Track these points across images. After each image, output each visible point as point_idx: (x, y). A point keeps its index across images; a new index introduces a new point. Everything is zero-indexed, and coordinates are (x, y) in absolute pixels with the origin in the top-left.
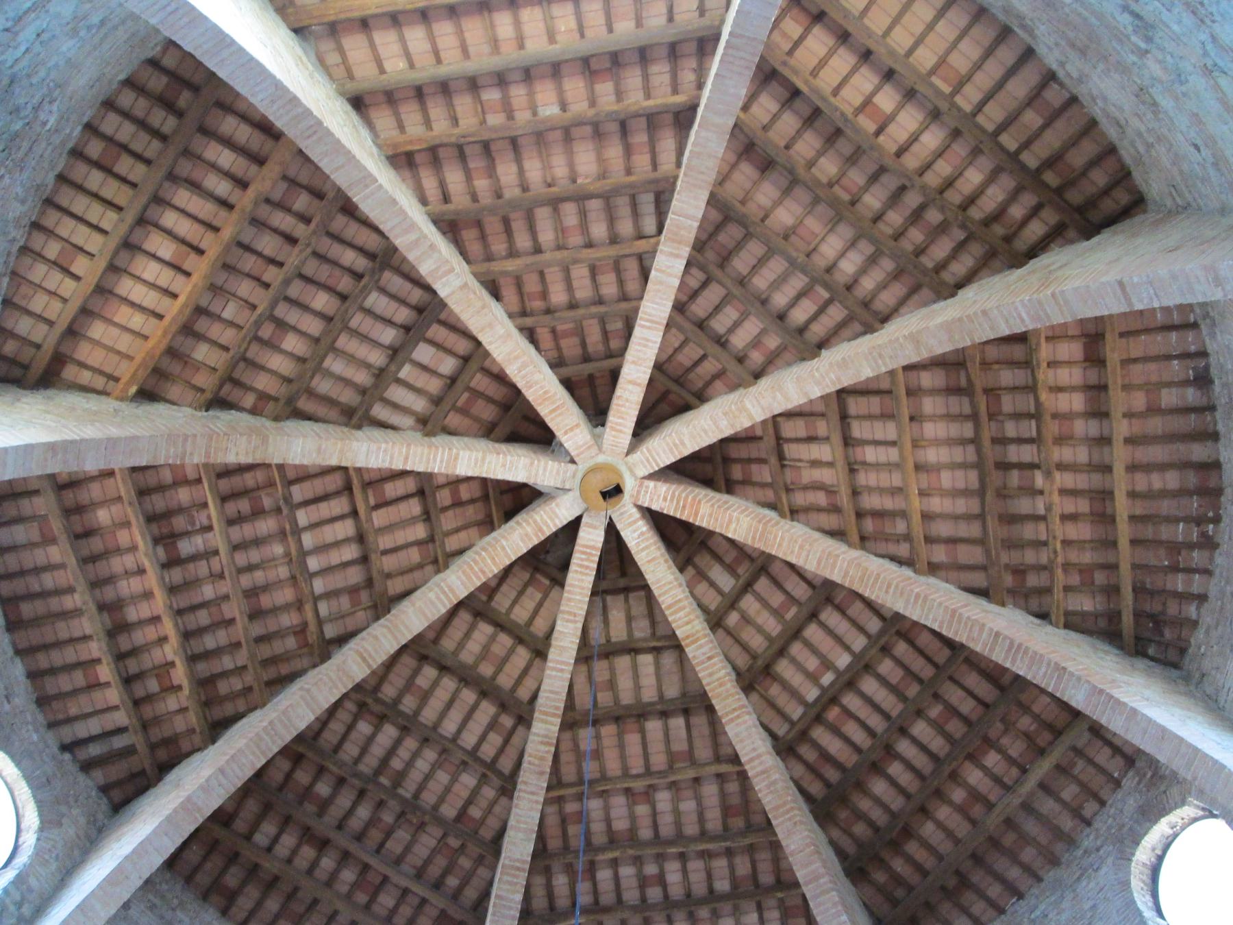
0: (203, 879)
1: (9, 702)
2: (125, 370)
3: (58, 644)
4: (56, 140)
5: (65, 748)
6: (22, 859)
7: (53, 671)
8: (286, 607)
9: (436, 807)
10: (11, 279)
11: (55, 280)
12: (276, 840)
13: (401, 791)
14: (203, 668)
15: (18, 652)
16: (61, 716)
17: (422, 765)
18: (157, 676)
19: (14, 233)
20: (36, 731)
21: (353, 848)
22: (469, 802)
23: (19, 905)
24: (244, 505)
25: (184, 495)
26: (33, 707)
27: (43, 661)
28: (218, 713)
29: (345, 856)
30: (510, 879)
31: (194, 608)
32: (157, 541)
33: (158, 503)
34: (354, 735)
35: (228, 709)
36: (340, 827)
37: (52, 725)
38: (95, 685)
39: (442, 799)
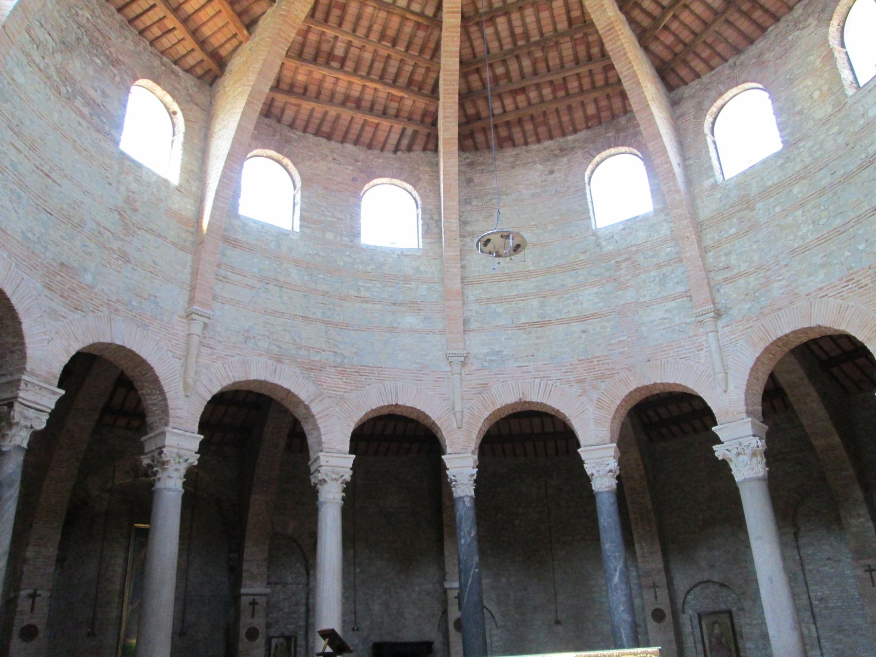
0: (493, 143)
1: (358, 161)
2: (232, 29)
3: (349, 128)
4: (98, 11)
5: (396, 151)
6: (419, 202)
7: (359, 136)
8: (401, 25)
9: (555, 30)
10: (165, 55)
11: (172, 38)
12: (503, 106)
13: (533, 39)
14: (403, 81)
15: (342, 142)
16: (381, 145)
17: (530, 19)
18: (391, 100)
19: (141, 48)
20: (378, 158)
21: (537, 80)
22: (568, 12)
23: (432, 218)
24: (336, 12)
25: (313, 37)
26: (369, 152)
27: (352, 136)
28: (427, 90)
29: (538, 86)
30: (609, 38)
31: (371, 66)
32: (327, 64)
33: (309, 51)
34: (489, 38)
35: (430, 82)
36: (523, 77)
37: (382, 150)
38: (377, 126)
39: (554, 24)
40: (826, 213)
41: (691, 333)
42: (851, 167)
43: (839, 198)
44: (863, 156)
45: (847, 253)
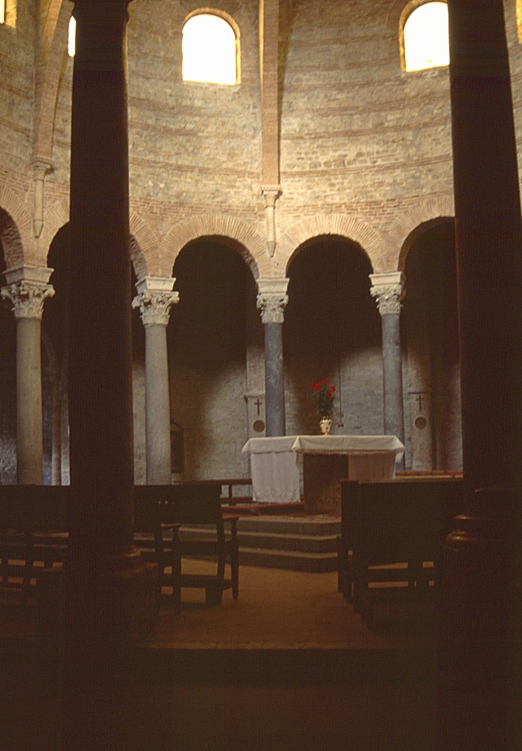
40: (145, 145)
41: (23, 171)
42: (171, 126)
43: (156, 140)
44: (183, 126)
45: (150, 183)
